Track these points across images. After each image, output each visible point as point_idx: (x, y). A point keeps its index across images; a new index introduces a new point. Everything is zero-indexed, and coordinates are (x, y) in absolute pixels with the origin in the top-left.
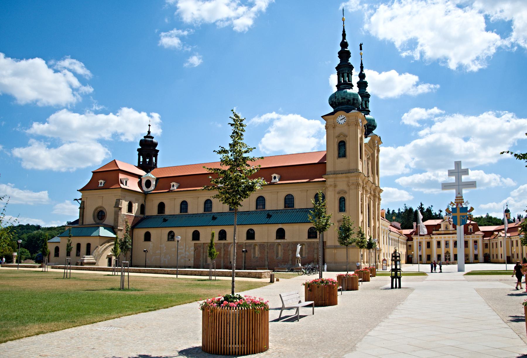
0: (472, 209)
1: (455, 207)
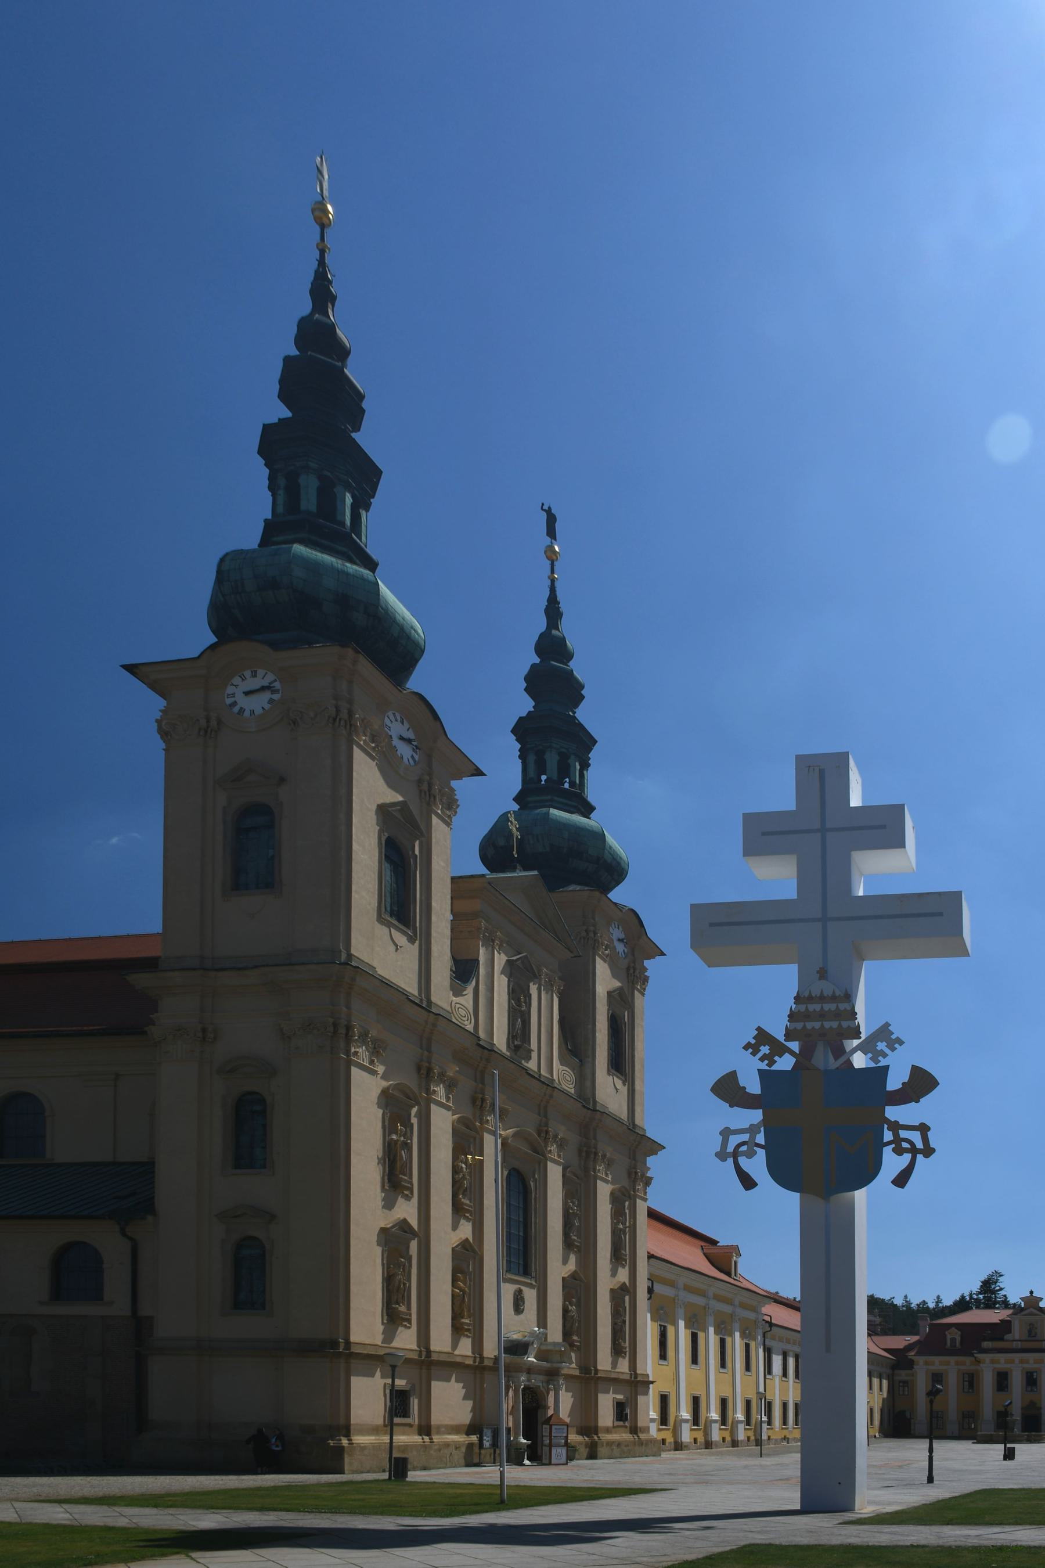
0: (921, 1084)
1: (785, 1063)
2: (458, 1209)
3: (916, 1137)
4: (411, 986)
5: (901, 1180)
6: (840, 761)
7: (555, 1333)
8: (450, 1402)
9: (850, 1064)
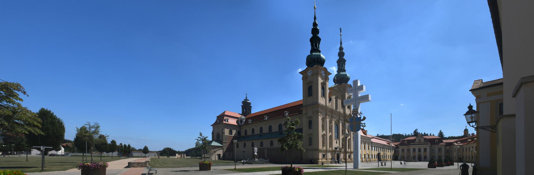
0: (364, 118)
2: (330, 131)
4: (324, 104)
6: (357, 80)
7: (341, 146)
8: (329, 156)
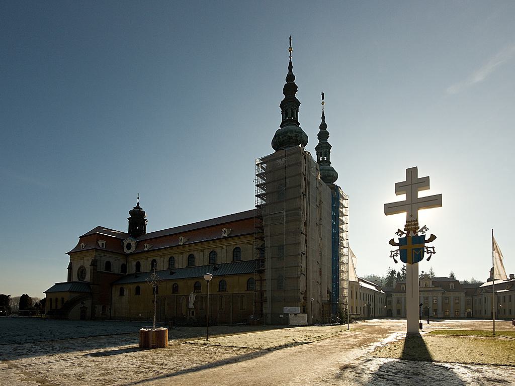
0: (433, 238)
1: (404, 236)
3: (432, 250)
5: (428, 259)
9: (417, 234)
